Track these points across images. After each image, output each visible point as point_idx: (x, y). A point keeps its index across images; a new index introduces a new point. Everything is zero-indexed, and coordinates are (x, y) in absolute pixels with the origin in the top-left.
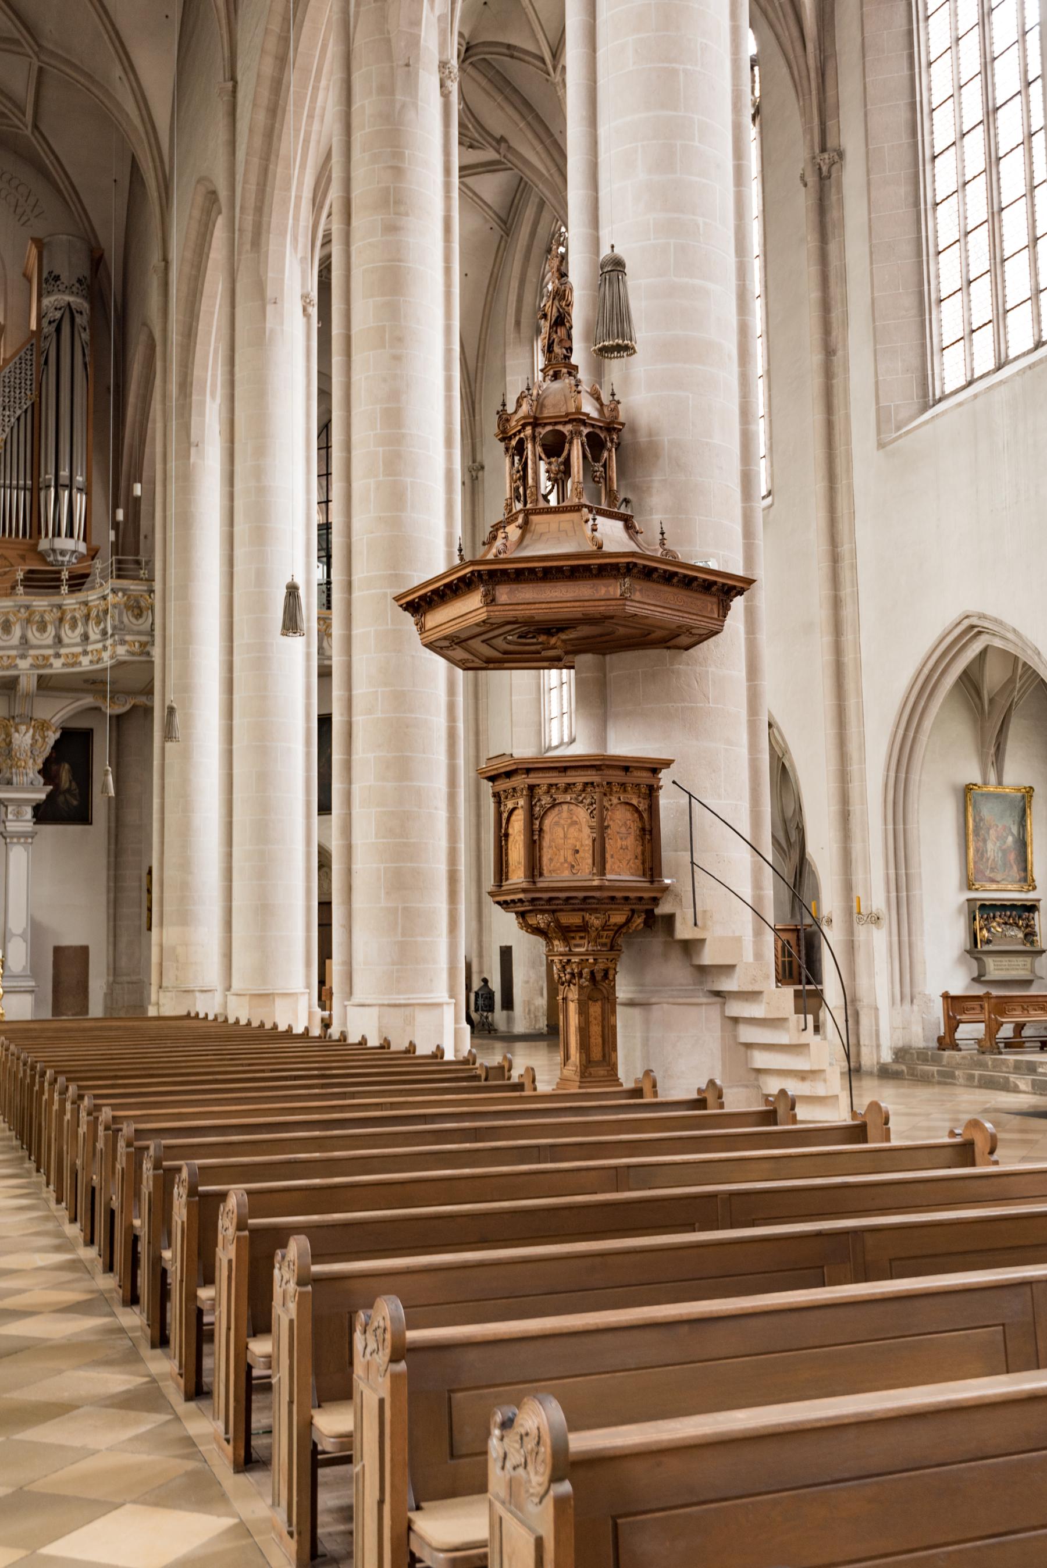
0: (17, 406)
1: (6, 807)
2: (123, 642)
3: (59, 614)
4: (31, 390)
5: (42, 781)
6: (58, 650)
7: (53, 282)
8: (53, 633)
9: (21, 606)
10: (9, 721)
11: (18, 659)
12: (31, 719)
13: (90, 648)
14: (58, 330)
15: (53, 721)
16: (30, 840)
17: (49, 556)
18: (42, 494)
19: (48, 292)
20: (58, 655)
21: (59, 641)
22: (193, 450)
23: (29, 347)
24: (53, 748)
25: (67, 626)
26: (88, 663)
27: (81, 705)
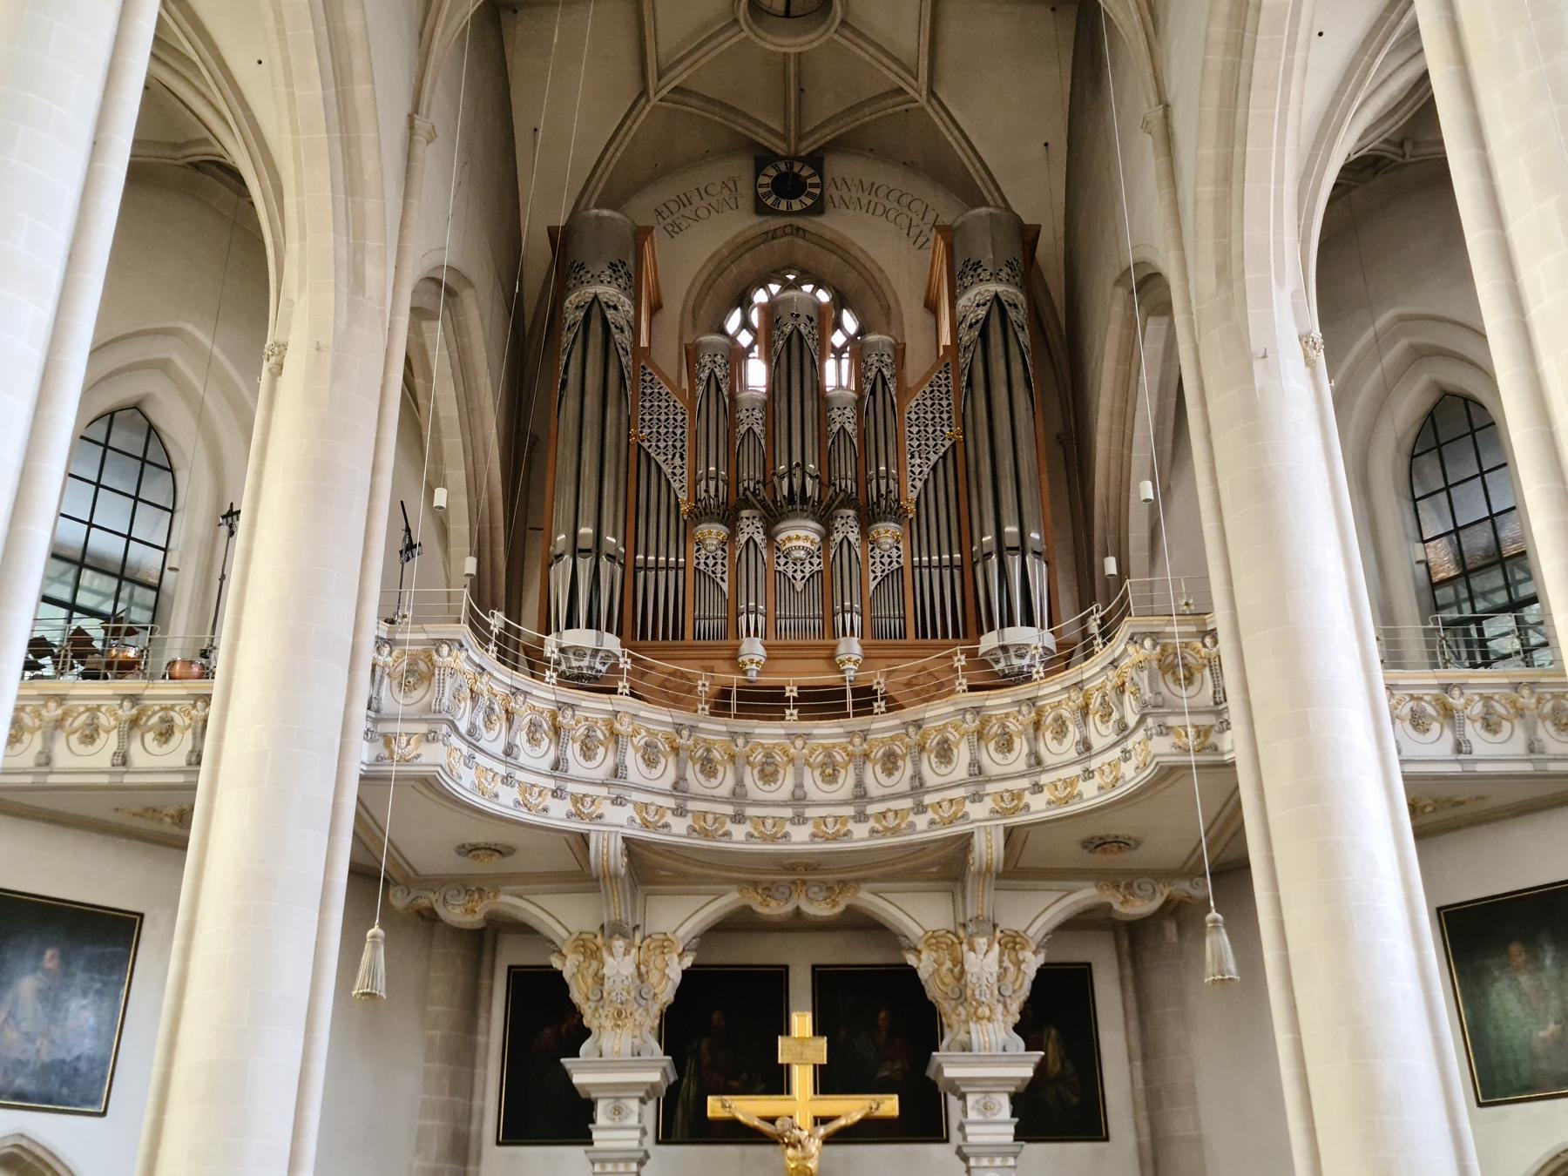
0: (932, 450)
1: (963, 1097)
2: (1165, 730)
3: (1033, 714)
4: (949, 426)
5: (1022, 1044)
6: (1036, 779)
7: (972, 273)
8: (1026, 750)
9: (965, 711)
10: (955, 934)
11: (967, 802)
12: (995, 926)
13: (1094, 764)
14: (984, 335)
15: (1031, 932)
16: (1011, 1161)
17: (997, 662)
18: (979, 568)
19: (966, 287)
20: (1037, 788)
21: (1037, 761)
22: (1257, 366)
23: (943, 369)
24: (1034, 983)
25: (1049, 735)
26: (1096, 792)
27: (1076, 902)
